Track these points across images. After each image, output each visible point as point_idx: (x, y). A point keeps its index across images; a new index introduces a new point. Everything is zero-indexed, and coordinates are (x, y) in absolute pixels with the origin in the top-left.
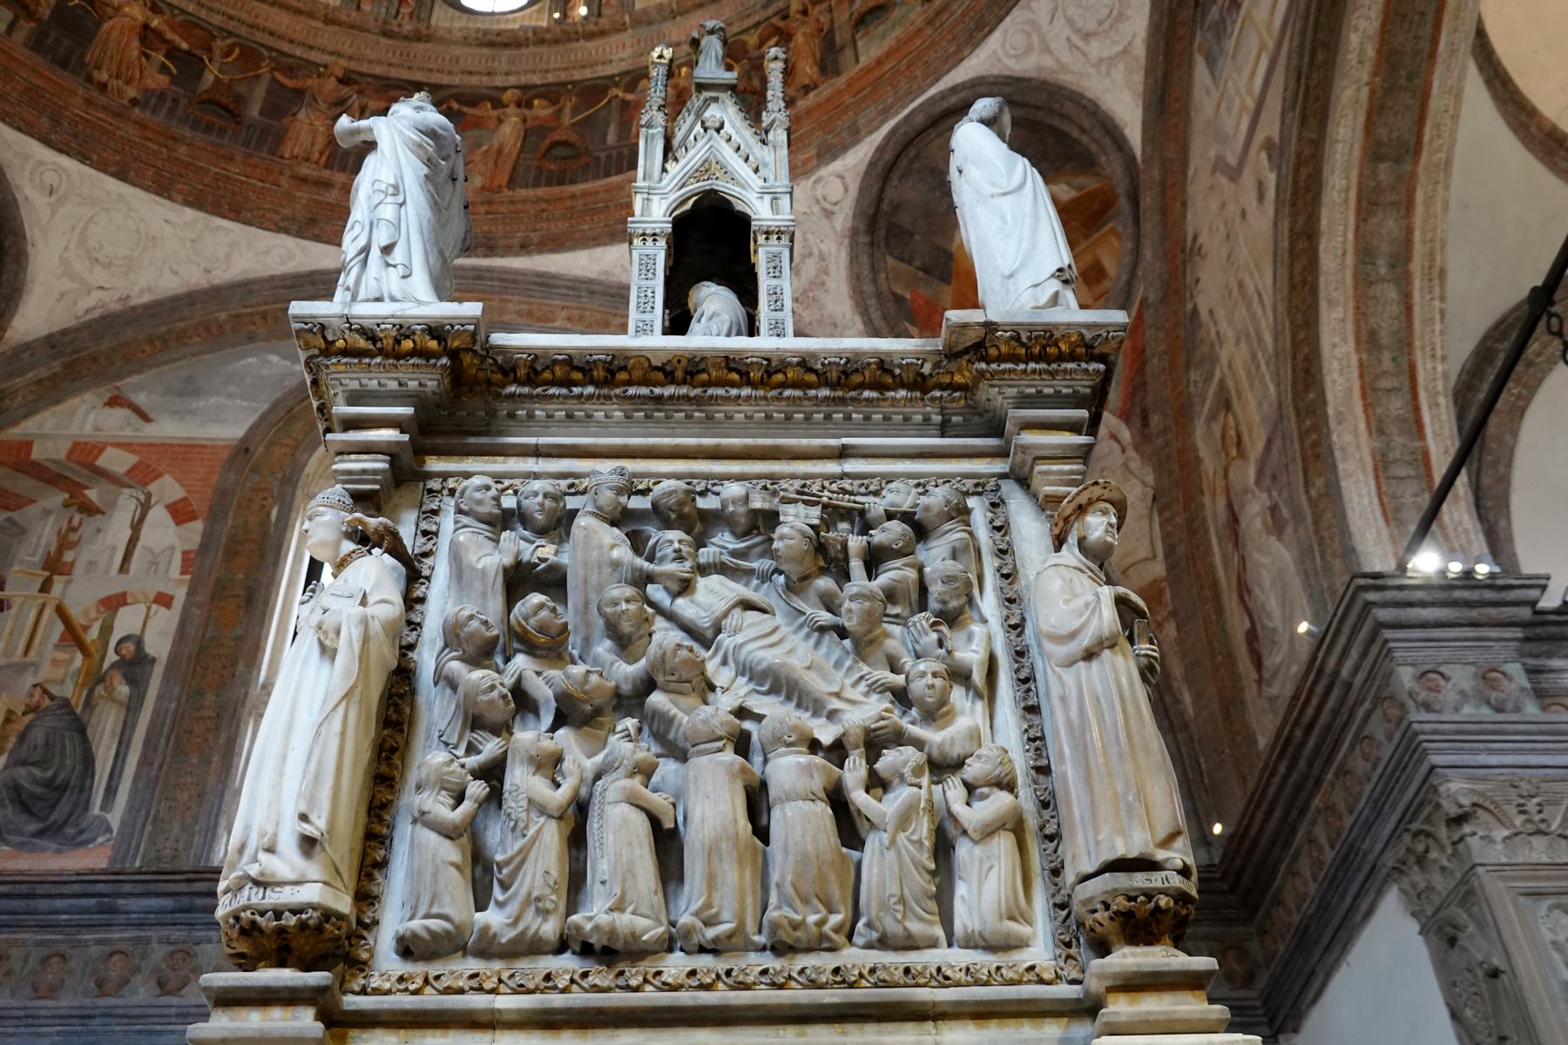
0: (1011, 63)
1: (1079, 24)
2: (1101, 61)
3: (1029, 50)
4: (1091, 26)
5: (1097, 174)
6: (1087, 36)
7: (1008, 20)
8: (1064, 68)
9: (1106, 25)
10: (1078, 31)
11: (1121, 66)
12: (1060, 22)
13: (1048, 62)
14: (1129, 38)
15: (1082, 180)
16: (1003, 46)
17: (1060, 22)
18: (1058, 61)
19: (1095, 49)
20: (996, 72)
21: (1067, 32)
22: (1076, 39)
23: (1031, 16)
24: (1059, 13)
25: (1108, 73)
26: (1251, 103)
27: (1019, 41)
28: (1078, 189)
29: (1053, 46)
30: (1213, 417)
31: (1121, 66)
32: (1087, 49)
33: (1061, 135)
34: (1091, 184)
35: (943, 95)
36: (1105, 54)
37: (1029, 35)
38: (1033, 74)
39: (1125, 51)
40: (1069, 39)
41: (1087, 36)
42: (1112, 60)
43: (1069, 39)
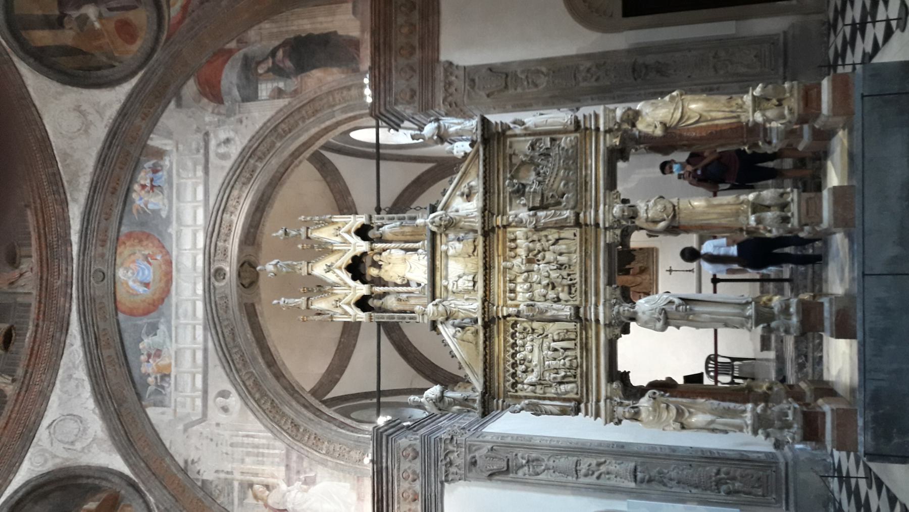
0: (40, 469)
1: (66, 440)
2: (83, 448)
3: (46, 461)
4: (72, 438)
5: (105, 490)
6: (72, 443)
7: (29, 454)
8: (67, 460)
9: (80, 435)
10: (67, 443)
11: (95, 445)
12: (56, 444)
13: (58, 461)
14: (94, 434)
15: (98, 496)
16: (32, 464)
17: (56, 444)
18: (63, 458)
19: (78, 446)
20: (34, 476)
21: (62, 445)
22: (66, 446)
23: (41, 448)
24: (55, 440)
25: (89, 451)
26: (200, 393)
27: (40, 460)
28: (99, 500)
29: (57, 454)
30: (242, 499)
31: (95, 445)
32: (74, 448)
33: (79, 486)
34: (103, 496)
35: (11, 497)
36: (85, 445)
37: (43, 455)
38: (54, 468)
39: (94, 440)
40: (64, 448)
41: (72, 443)
42: (89, 445)
43: (64, 448)
